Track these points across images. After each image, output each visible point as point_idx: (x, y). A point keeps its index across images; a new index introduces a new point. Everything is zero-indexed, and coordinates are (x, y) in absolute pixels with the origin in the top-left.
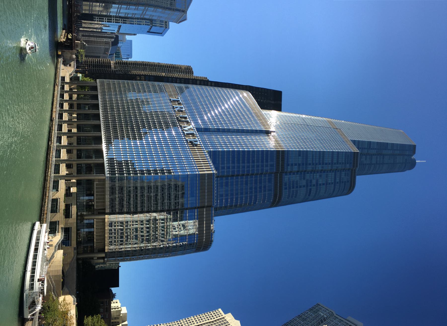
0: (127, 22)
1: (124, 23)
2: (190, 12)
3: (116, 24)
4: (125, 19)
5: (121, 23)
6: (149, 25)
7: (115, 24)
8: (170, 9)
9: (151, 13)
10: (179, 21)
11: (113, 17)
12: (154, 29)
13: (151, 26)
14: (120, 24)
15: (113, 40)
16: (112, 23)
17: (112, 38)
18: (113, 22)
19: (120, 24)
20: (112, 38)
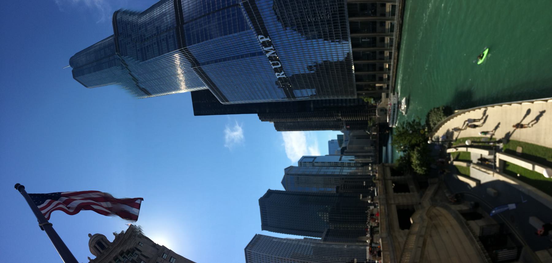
0: (333, 164)
1: (337, 163)
2: (283, 174)
3: (343, 162)
4: (336, 165)
5: (339, 163)
6: (316, 162)
7: (345, 162)
8: (299, 175)
9: (315, 171)
10: (291, 167)
11: (346, 167)
12: (311, 160)
13: (313, 162)
14: (340, 162)
15: (345, 151)
16: (347, 162)
17: (346, 152)
18: (346, 163)
19: (340, 162)
20: (346, 152)
